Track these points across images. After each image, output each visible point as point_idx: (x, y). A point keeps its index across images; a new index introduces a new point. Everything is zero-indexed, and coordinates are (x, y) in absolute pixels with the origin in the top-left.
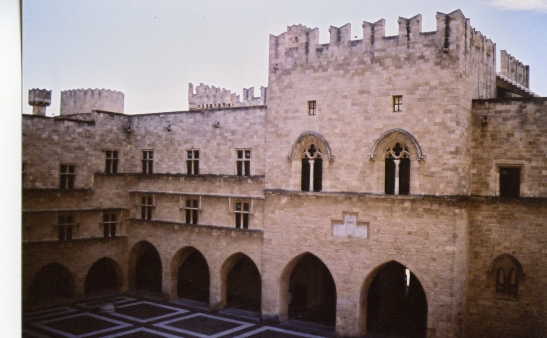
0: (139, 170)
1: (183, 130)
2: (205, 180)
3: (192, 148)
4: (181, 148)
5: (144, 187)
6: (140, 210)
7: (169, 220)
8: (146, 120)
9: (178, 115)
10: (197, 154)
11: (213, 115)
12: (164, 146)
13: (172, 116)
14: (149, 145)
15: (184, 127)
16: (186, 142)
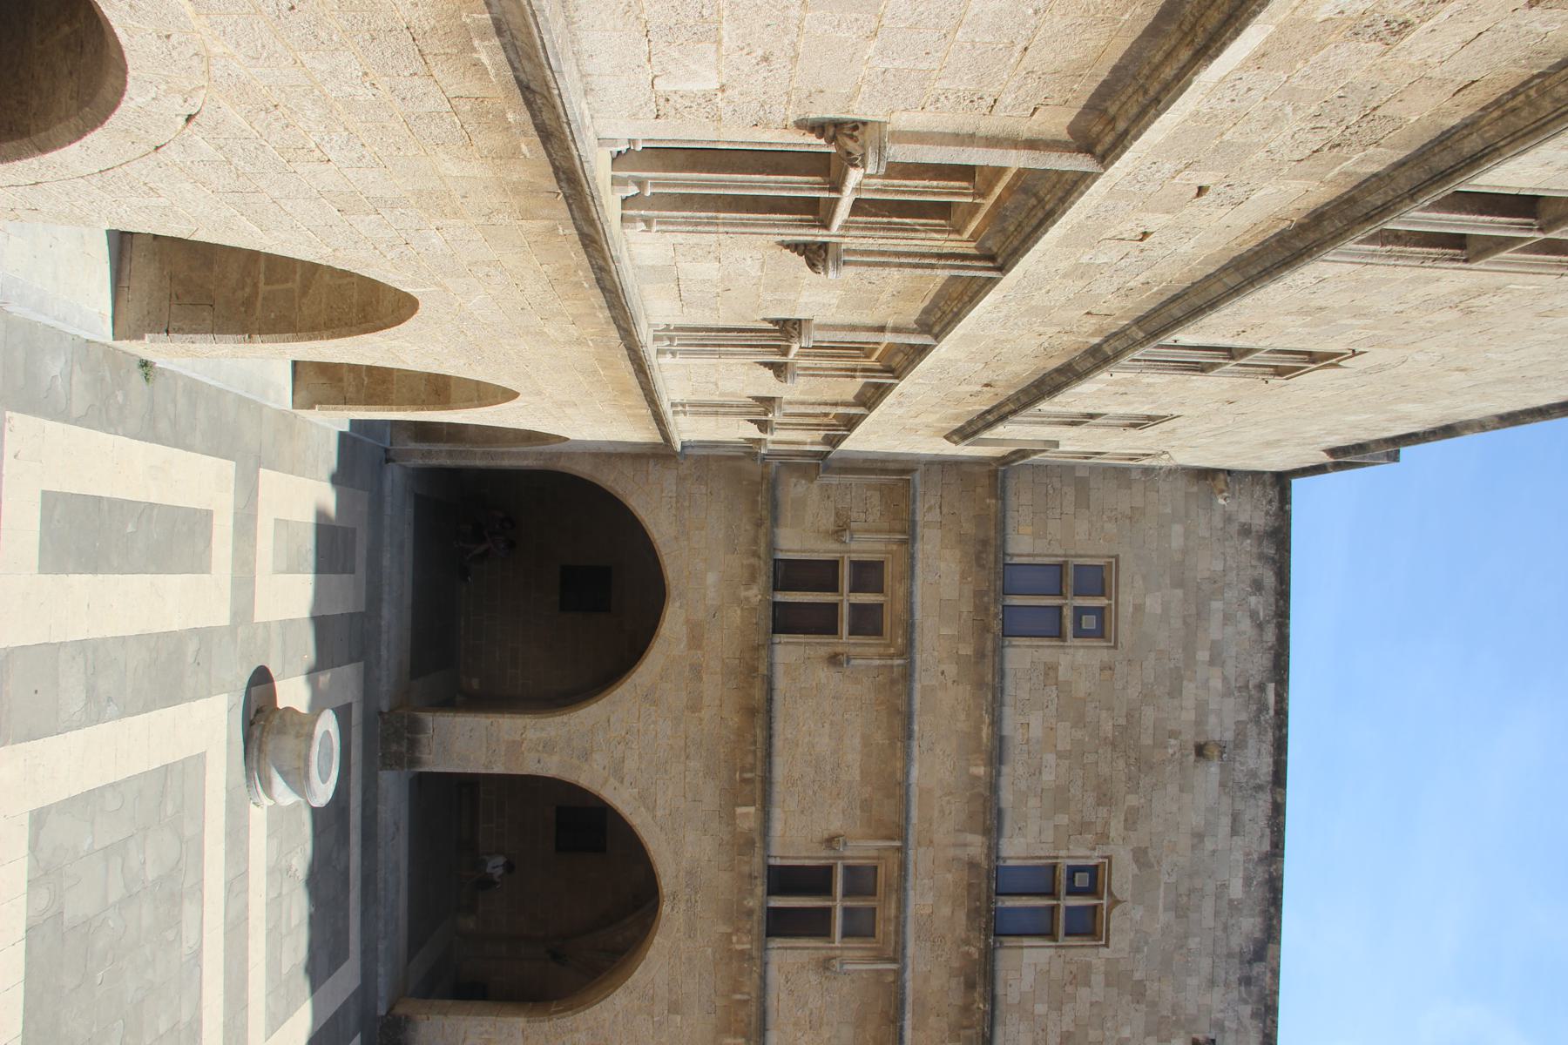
0: (1024, 544)
1: (1199, 836)
2: (970, 986)
3: (1115, 902)
4: (1116, 828)
5: (939, 581)
6: (823, 550)
7: (779, 772)
8: (1257, 586)
9: (1264, 801)
10: (1087, 926)
11: (1246, 1010)
12: (1129, 716)
13: (1265, 767)
14: (1139, 608)
15: (1209, 845)
16: (1140, 856)
